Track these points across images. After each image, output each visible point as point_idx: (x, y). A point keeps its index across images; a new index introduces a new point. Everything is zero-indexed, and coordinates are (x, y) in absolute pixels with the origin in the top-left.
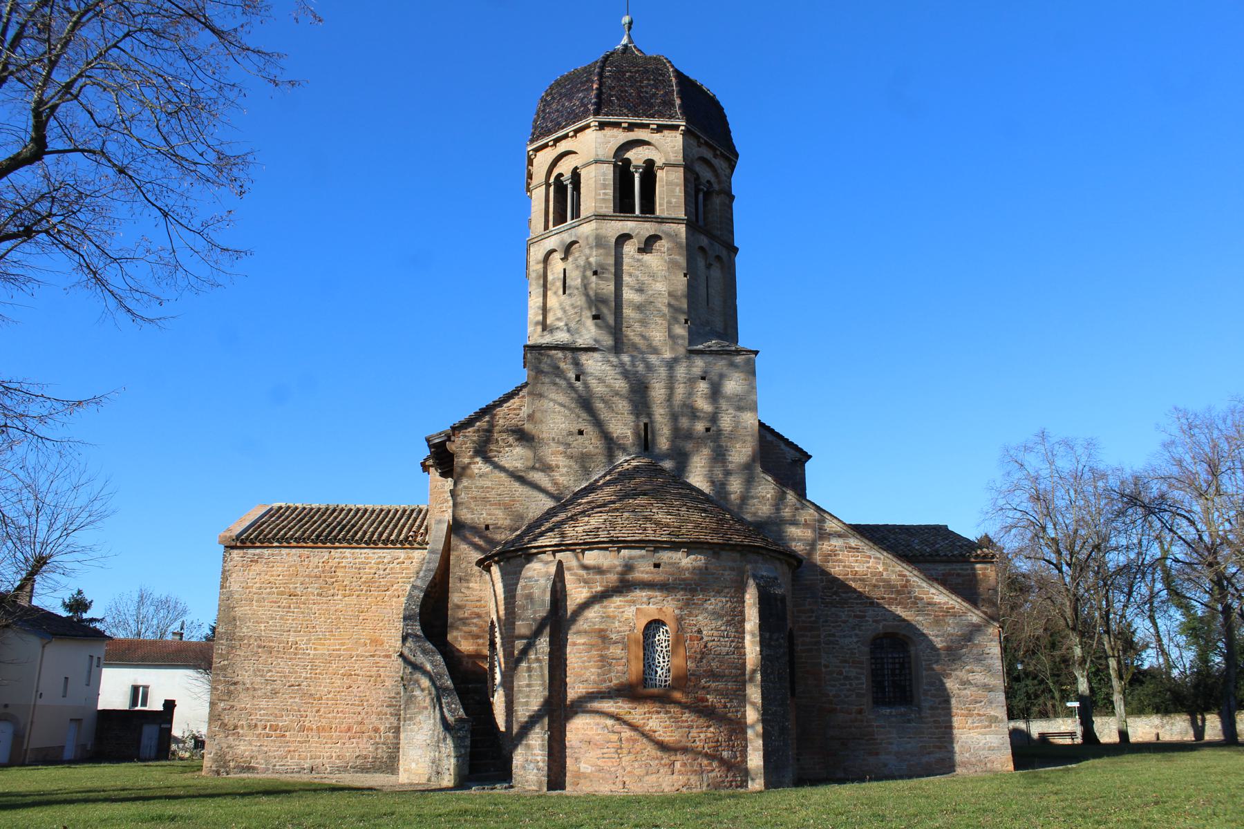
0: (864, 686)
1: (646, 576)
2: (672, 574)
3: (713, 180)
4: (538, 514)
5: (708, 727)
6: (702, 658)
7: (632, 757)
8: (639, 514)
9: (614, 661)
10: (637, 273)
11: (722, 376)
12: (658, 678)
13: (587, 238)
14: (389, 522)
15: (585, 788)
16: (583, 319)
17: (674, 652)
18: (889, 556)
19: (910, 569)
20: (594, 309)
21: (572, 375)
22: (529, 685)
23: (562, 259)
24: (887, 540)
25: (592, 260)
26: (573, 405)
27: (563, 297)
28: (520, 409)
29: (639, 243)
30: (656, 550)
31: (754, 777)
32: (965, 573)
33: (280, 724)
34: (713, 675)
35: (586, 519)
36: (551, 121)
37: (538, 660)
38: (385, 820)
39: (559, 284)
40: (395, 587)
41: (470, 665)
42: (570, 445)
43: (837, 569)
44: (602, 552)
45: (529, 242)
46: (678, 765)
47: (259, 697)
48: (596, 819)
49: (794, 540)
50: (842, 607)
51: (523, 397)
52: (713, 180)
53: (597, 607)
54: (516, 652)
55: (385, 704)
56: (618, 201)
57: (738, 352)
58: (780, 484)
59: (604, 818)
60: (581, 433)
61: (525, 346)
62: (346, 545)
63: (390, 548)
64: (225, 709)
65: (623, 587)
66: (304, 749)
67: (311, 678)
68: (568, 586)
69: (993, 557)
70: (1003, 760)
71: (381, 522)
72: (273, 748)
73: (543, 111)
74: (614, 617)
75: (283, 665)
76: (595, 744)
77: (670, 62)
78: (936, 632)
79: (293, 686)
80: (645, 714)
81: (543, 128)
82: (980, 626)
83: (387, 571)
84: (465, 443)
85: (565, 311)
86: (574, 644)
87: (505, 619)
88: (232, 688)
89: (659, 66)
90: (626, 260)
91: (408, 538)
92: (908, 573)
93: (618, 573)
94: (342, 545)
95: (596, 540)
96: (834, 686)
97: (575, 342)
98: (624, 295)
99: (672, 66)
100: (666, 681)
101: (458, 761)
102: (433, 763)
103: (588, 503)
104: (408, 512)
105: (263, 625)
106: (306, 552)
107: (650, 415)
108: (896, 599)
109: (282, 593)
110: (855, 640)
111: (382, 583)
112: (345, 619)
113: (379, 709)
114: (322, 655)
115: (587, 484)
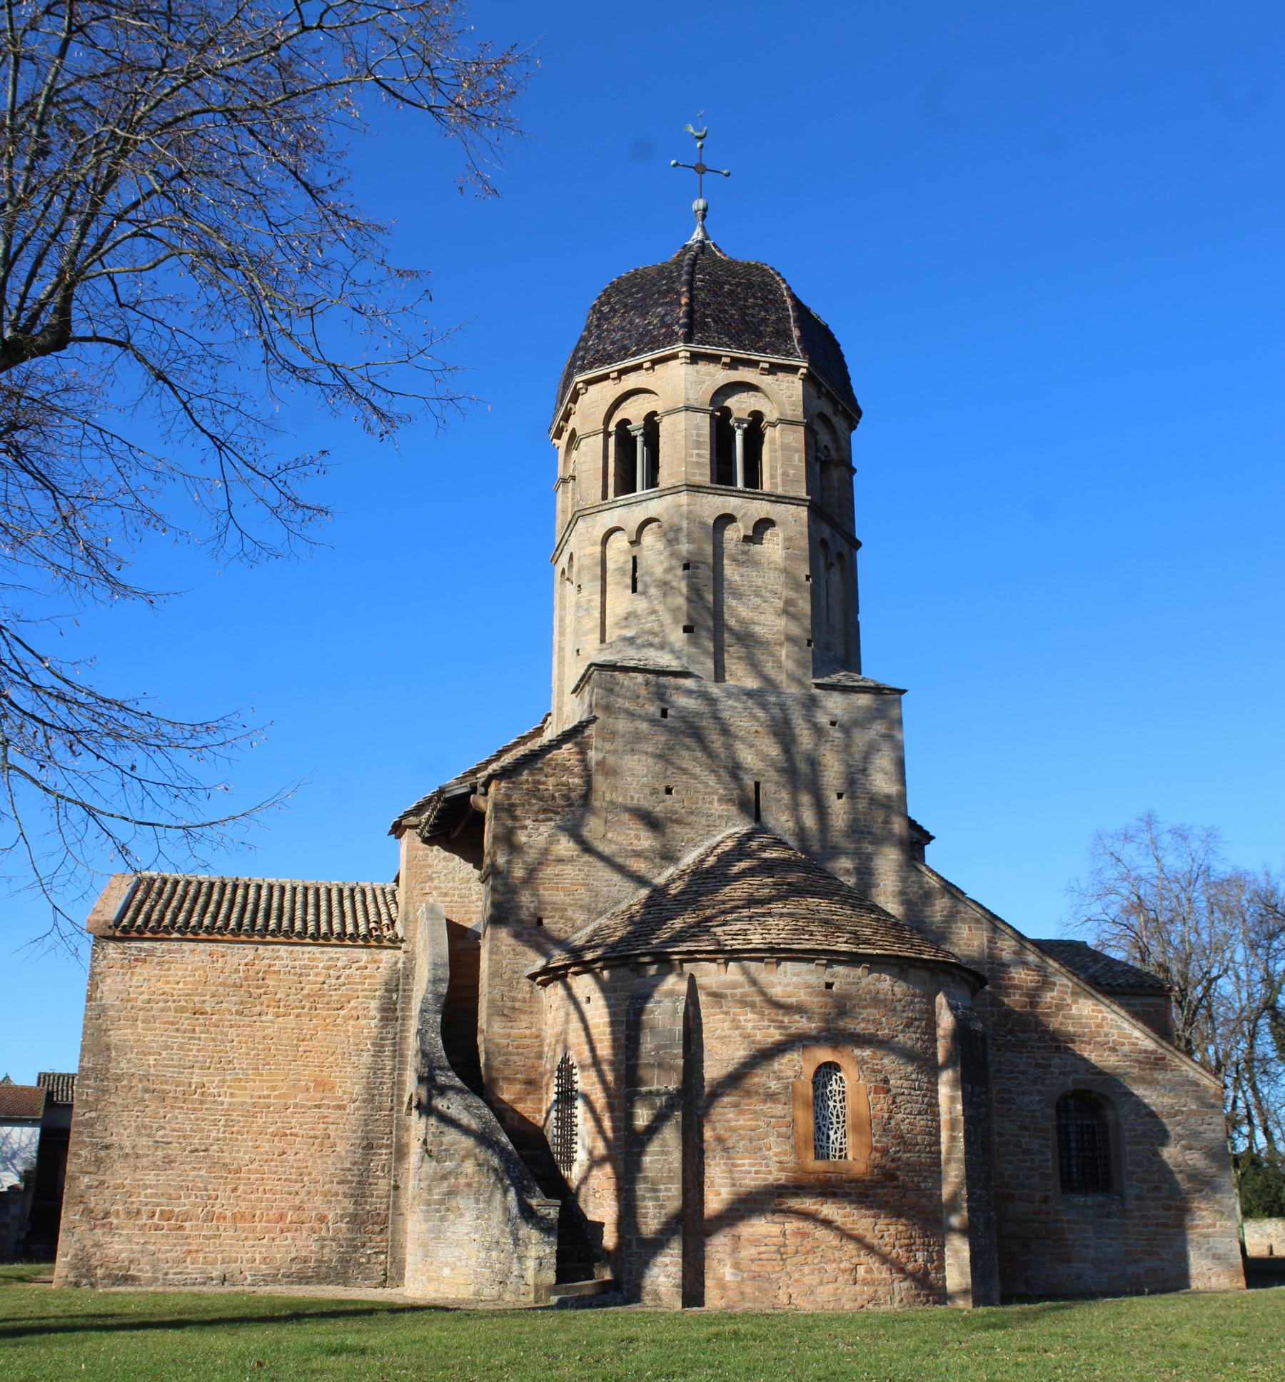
0: (1050, 1164)
3: (831, 445)
12: (831, 1145)
29: (746, 528)
30: (830, 964)
33: (176, 1210)
40: (353, 1003)
41: (516, 1123)
47: (144, 1168)
52: (831, 445)
55: (336, 1180)
62: (282, 939)
63: (243, 942)
64: (91, 1187)
66: (212, 1249)
68: (703, 1012)
72: (164, 1246)
75: (182, 1119)
79: (196, 1150)
83: (342, 979)
88: (103, 1153)
94: (275, 940)
96: (1010, 1162)
105: (152, 1058)
106: (220, 948)
109: (182, 1010)
110: (1037, 1098)
111: (334, 998)
112: (278, 1050)
113: (327, 1187)
114: (242, 1104)
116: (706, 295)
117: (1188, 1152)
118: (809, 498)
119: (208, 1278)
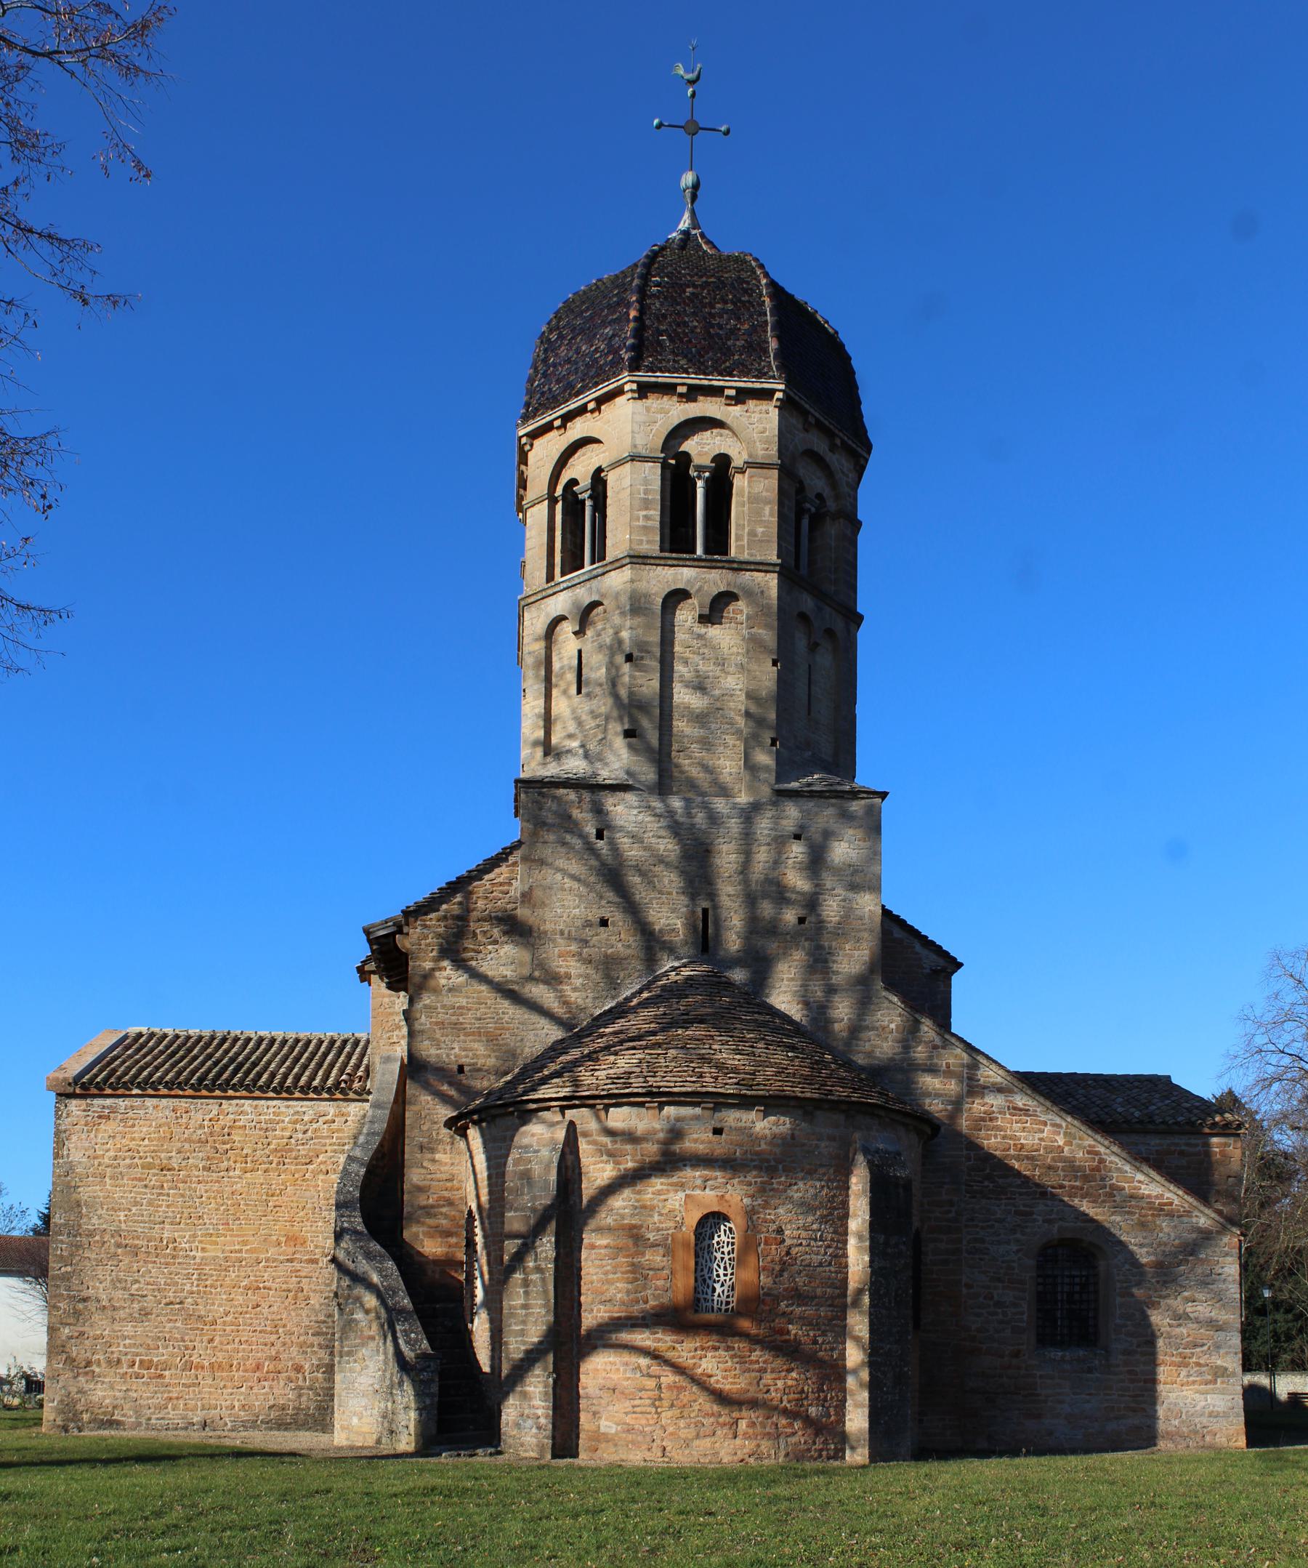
0: (1025, 1317)
1: (701, 1147)
2: (741, 1145)
4: (539, 1049)
5: (790, 1371)
6: (782, 1271)
7: (676, 1412)
8: (693, 1051)
9: (651, 1273)
10: (696, 658)
11: (828, 835)
13: (617, 595)
14: (310, 1059)
15: (608, 1455)
16: (609, 737)
17: (741, 1261)
18: (1076, 1122)
19: (1106, 1143)
20: (626, 720)
21: (591, 830)
22: (525, 1306)
23: (575, 633)
24: (1073, 1097)
25: (625, 635)
26: (592, 879)
27: (577, 699)
28: (510, 884)
29: (701, 606)
31: (854, 1444)
32: (1192, 1150)
34: (799, 1296)
35: (612, 1058)
36: (558, 382)
37: (538, 1269)
38: (318, 1500)
39: (571, 677)
42: (587, 942)
43: (993, 1140)
44: (635, 1110)
45: (523, 603)
46: (743, 1425)
47: (122, 1320)
48: (622, 1502)
49: (928, 1095)
50: (996, 1199)
51: (515, 864)
53: (627, 1193)
54: (506, 1258)
55: (310, 1332)
56: (667, 531)
57: (855, 794)
58: (911, 1007)
59: (634, 1501)
60: (604, 923)
61: (517, 781)
64: (71, 1337)
65: (665, 1163)
66: (191, 1396)
67: (199, 1292)
69: (1240, 1126)
70: (1231, 1432)
71: (297, 1060)
72: (145, 1392)
73: (545, 361)
74: (652, 1208)
76: (623, 1393)
77: (762, 266)
78: (1139, 1240)
79: (171, 1303)
80: (696, 1350)
81: (543, 394)
82: (1210, 1232)
84: (426, 938)
85: (580, 724)
86: (593, 1247)
87: (490, 1208)
88: (81, 1306)
89: (744, 275)
90: (680, 636)
91: (340, 1083)
92: (1102, 1150)
93: (658, 1142)
95: (627, 1091)
97: (595, 775)
98: (676, 697)
99: (766, 275)
100: (728, 1303)
101: (420, 1415)
102: (384, 1417)
103: (615, 1033)
104: (338, 1044)
107: (712, 896)
108: (1082, 1189)
110: (1015, 1248)
113: (302, 1338)
115: (613, 1004)
116: (662, 304)
117: (1190, 1304)
118: (779, 561)
119: (189, 1423)
